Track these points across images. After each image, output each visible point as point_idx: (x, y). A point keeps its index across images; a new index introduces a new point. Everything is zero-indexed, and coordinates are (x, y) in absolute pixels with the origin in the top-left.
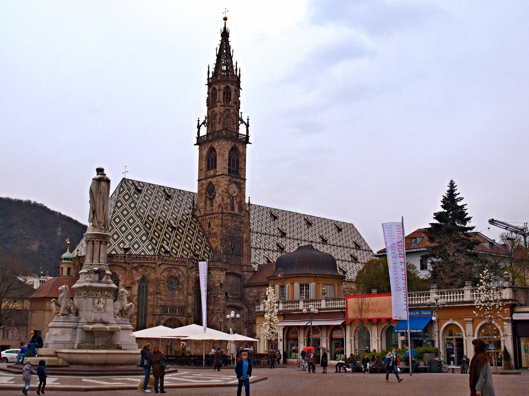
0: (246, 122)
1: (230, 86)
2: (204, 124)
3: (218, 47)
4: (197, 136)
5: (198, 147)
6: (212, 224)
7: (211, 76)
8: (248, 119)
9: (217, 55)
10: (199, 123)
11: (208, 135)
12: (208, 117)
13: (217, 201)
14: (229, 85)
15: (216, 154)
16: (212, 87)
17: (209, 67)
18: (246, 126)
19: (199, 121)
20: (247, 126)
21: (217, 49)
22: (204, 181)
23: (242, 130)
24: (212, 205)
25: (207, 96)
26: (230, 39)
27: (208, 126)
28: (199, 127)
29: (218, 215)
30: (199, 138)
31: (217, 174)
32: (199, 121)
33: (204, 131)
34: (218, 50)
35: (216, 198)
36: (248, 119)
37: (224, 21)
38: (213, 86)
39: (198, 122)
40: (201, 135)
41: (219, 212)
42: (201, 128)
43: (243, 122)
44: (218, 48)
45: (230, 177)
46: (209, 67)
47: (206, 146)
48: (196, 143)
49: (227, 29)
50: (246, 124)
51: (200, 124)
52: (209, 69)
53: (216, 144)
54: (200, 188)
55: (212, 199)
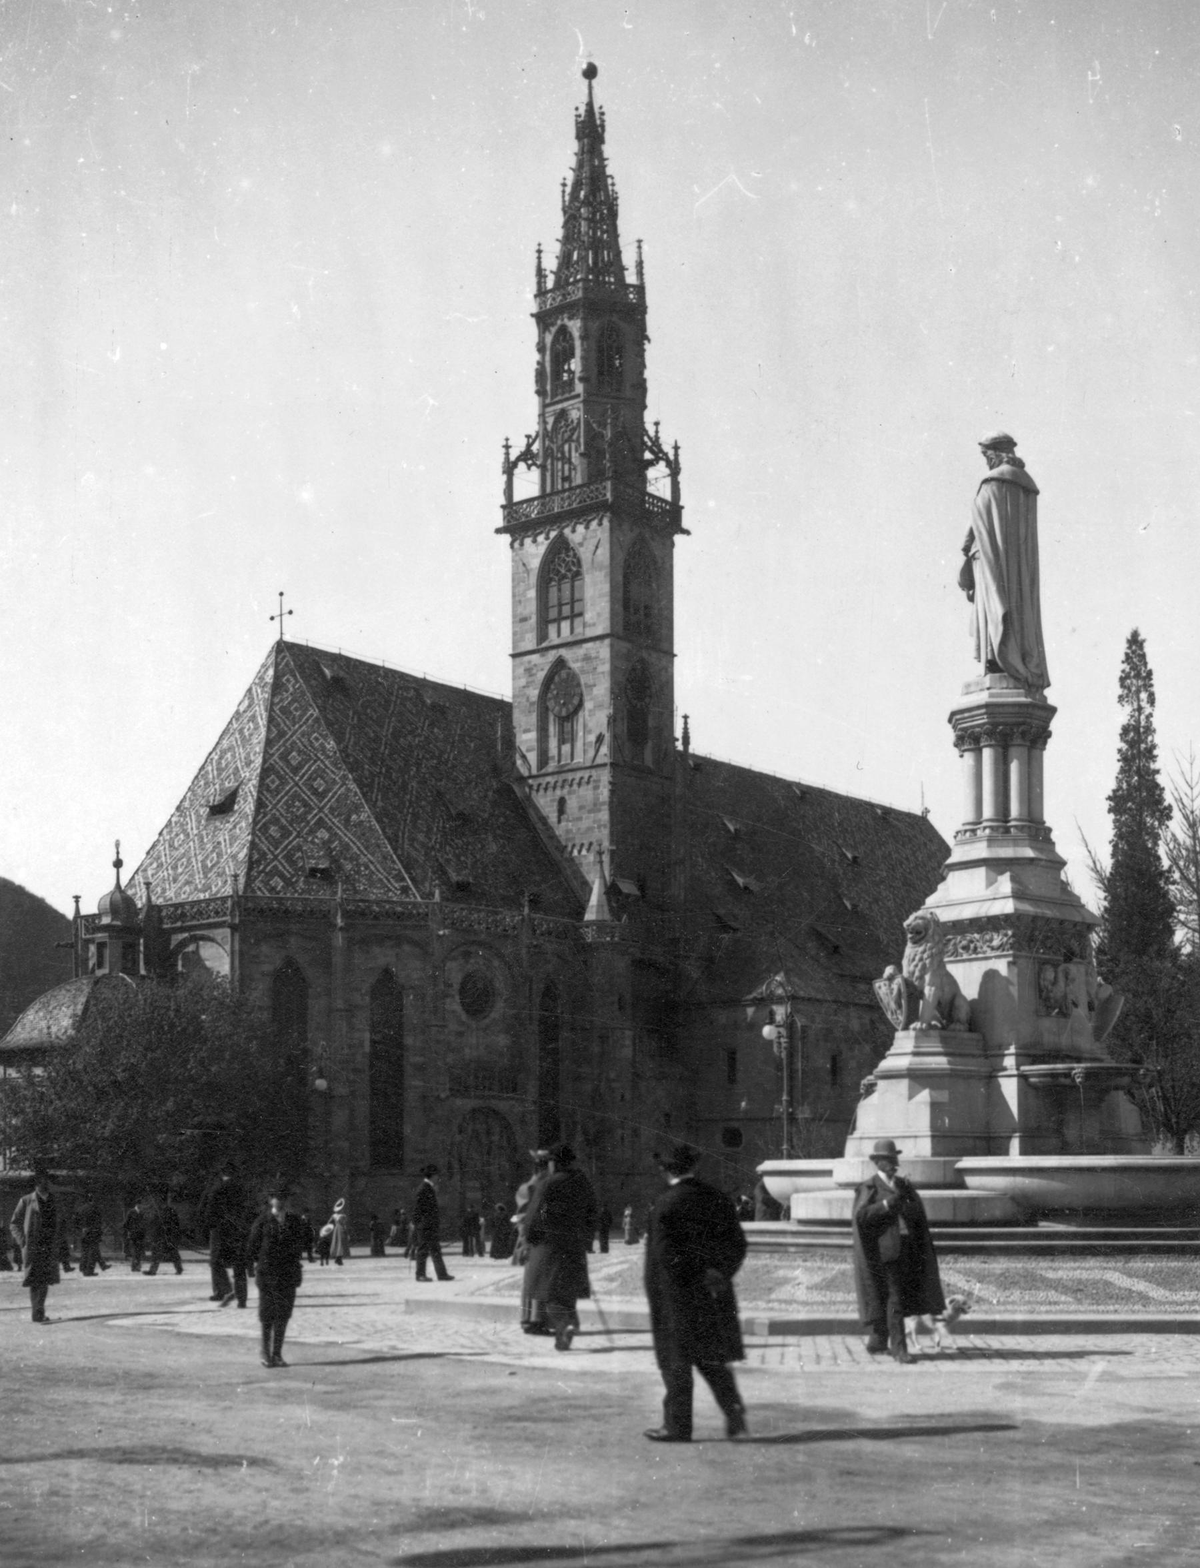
0: (671, 457)
1: (622, 325)
2: (525, 460)
3: (570, 177)
4: (503, 501)
5: (506, 538)
6: (572, 804)
7: (550, 283)
8: (676, 448)
9: (565, 211)
10: (507, 454)
11: (543, 496)
12: (546, 435)
13: (591, 725)
14: (615, 318)
15: (579, 563)
16: (553, 324)
17: (539, 252)
18: (667, 471)
19: (507, 447)
20: (675, 469)
21: (564, 185)
22: (535, 658)
23: (658, 481)
24: (567, 737)
25: (536, 357)
26: (608, 149)
27: (543, 468)
28: (509, 469)
29: (594, 772)
30: (510, 507)
31: (590, 633)
32: (507, 447)
33: (528, 484)
34: (568, 189)
35: (587, 713)
36: (676, 448)
37: (586, 82)
38: (559, 322)
39: (503, 450)
40: (517, 498)
41: (599, 761)
42: (516, 471)
43: (659, 454)
44: (569, 182)
45: (628, 645)
46: (539, 252)
47: (541, 538)
48: (500, 523)
49: (597, 110)
50: (669, 464)
51: (513, 458)
52: (539, 258)
53: (580, 529)
54: (523, 682)
55: (568, 718)
